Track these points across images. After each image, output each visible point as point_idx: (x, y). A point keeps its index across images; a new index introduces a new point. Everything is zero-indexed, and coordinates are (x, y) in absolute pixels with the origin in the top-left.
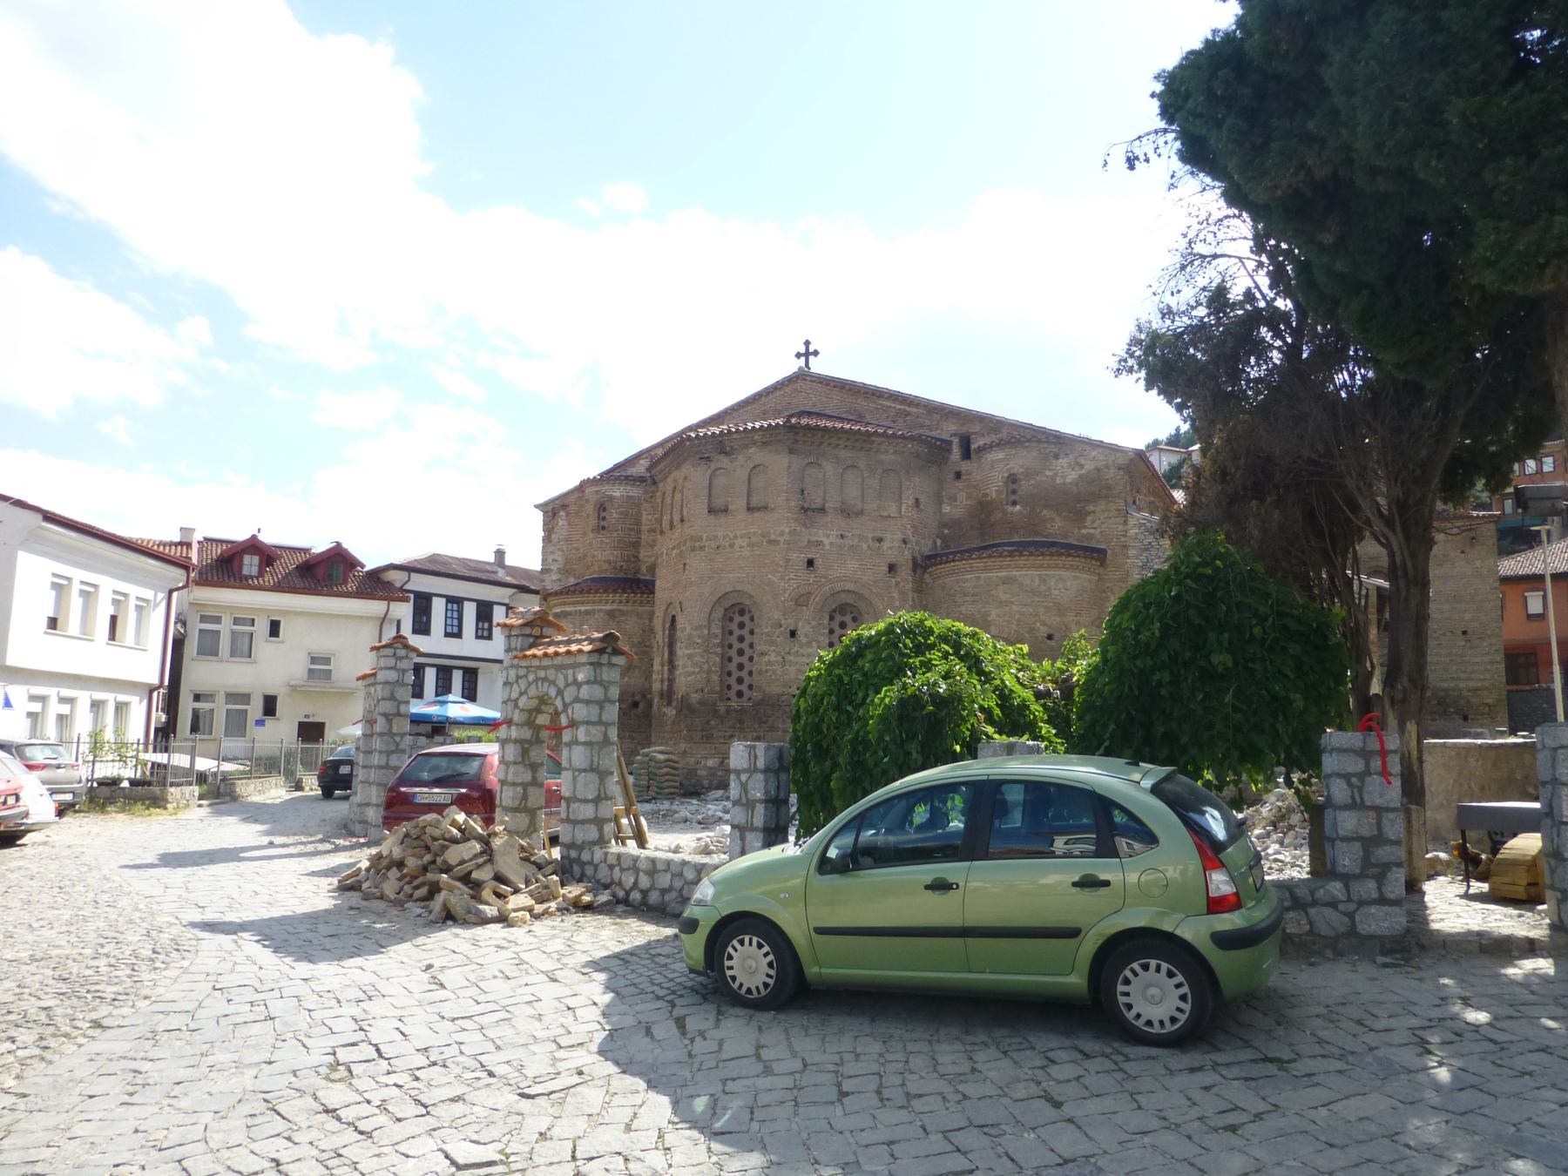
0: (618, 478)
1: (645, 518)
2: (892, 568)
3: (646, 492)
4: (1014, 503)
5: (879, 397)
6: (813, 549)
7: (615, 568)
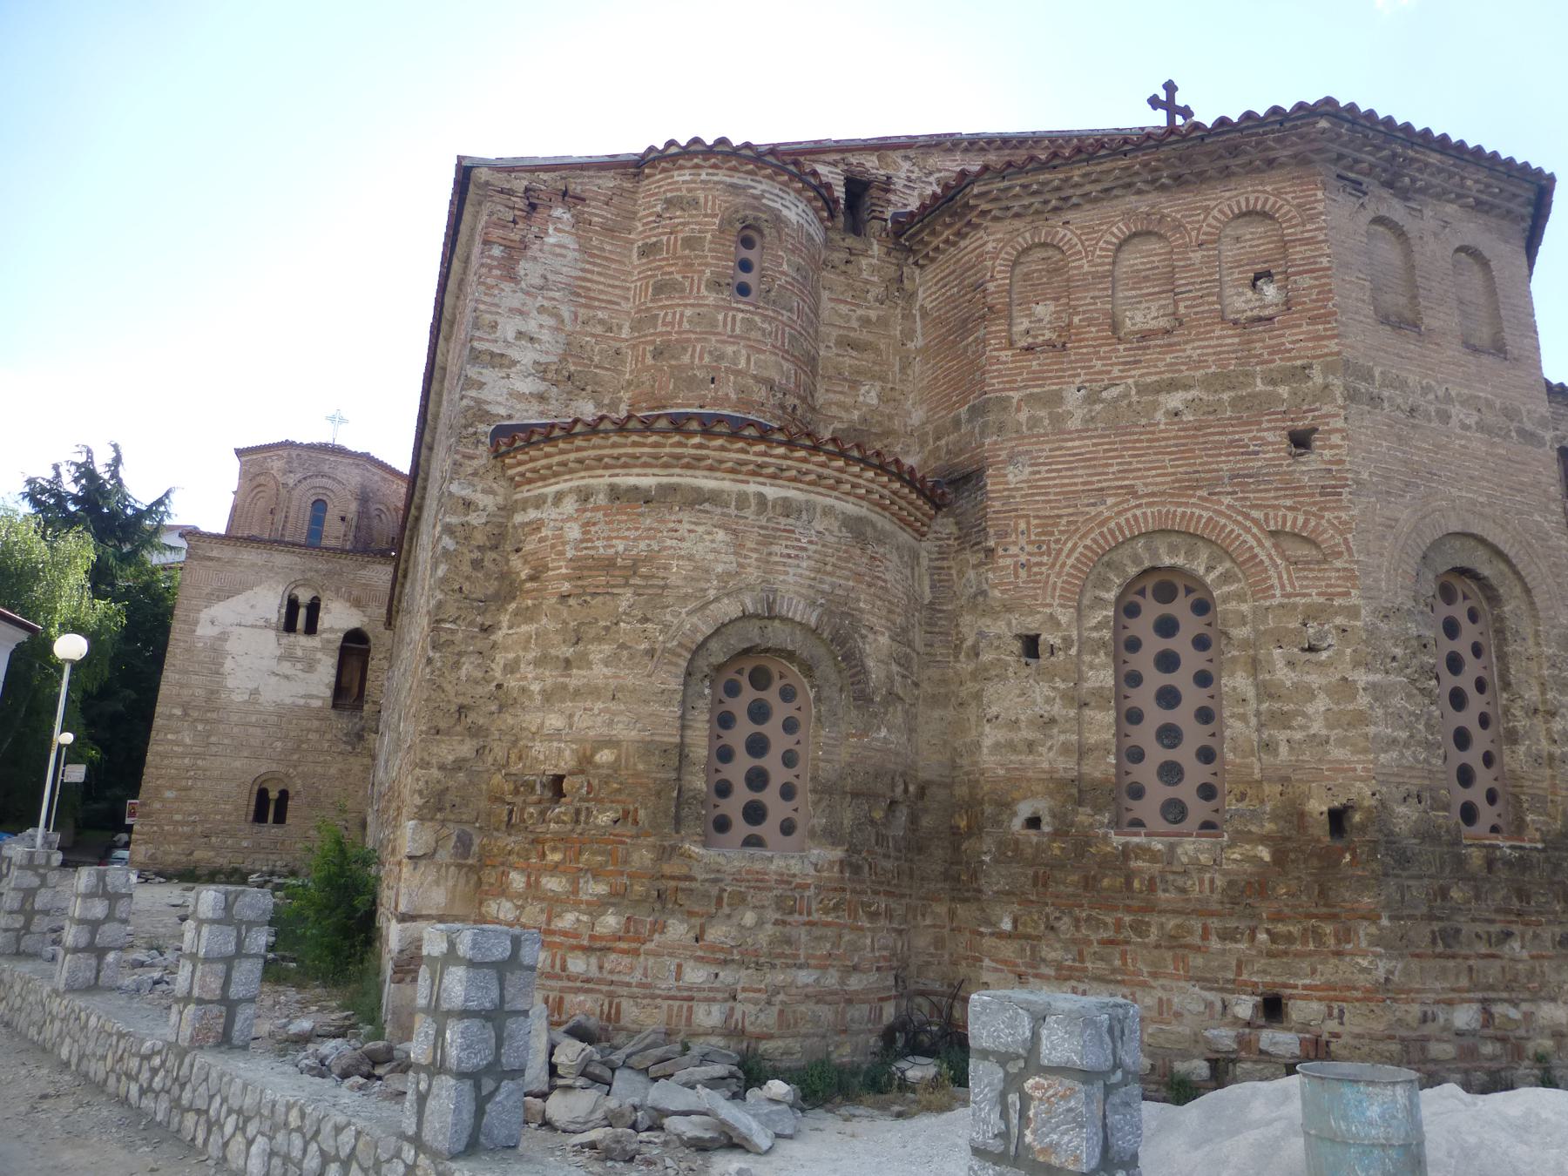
7: (782, 407)
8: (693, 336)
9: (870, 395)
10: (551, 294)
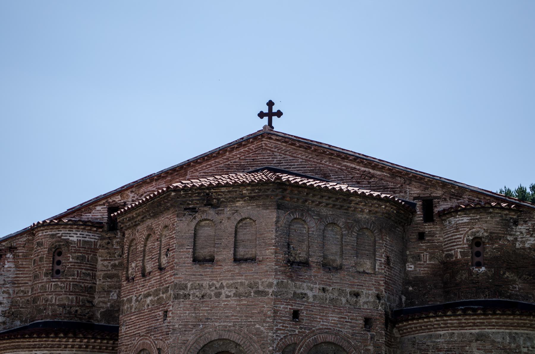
0: (75, 223)
1: (100, 264)
2: (368, 322)
3: (102, 238)
4: (479, 265)
5: (343, 158)
6: (298, 301)
7: (70, 313)
8: (40, 294)
9: (114, 296)
10: (6, 286)
